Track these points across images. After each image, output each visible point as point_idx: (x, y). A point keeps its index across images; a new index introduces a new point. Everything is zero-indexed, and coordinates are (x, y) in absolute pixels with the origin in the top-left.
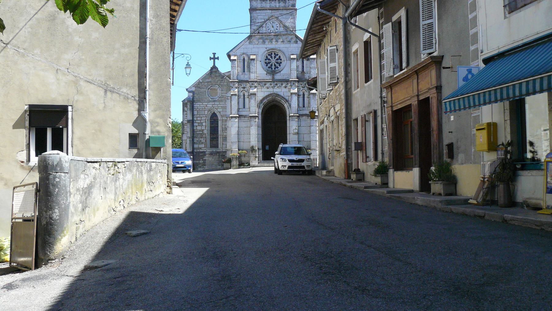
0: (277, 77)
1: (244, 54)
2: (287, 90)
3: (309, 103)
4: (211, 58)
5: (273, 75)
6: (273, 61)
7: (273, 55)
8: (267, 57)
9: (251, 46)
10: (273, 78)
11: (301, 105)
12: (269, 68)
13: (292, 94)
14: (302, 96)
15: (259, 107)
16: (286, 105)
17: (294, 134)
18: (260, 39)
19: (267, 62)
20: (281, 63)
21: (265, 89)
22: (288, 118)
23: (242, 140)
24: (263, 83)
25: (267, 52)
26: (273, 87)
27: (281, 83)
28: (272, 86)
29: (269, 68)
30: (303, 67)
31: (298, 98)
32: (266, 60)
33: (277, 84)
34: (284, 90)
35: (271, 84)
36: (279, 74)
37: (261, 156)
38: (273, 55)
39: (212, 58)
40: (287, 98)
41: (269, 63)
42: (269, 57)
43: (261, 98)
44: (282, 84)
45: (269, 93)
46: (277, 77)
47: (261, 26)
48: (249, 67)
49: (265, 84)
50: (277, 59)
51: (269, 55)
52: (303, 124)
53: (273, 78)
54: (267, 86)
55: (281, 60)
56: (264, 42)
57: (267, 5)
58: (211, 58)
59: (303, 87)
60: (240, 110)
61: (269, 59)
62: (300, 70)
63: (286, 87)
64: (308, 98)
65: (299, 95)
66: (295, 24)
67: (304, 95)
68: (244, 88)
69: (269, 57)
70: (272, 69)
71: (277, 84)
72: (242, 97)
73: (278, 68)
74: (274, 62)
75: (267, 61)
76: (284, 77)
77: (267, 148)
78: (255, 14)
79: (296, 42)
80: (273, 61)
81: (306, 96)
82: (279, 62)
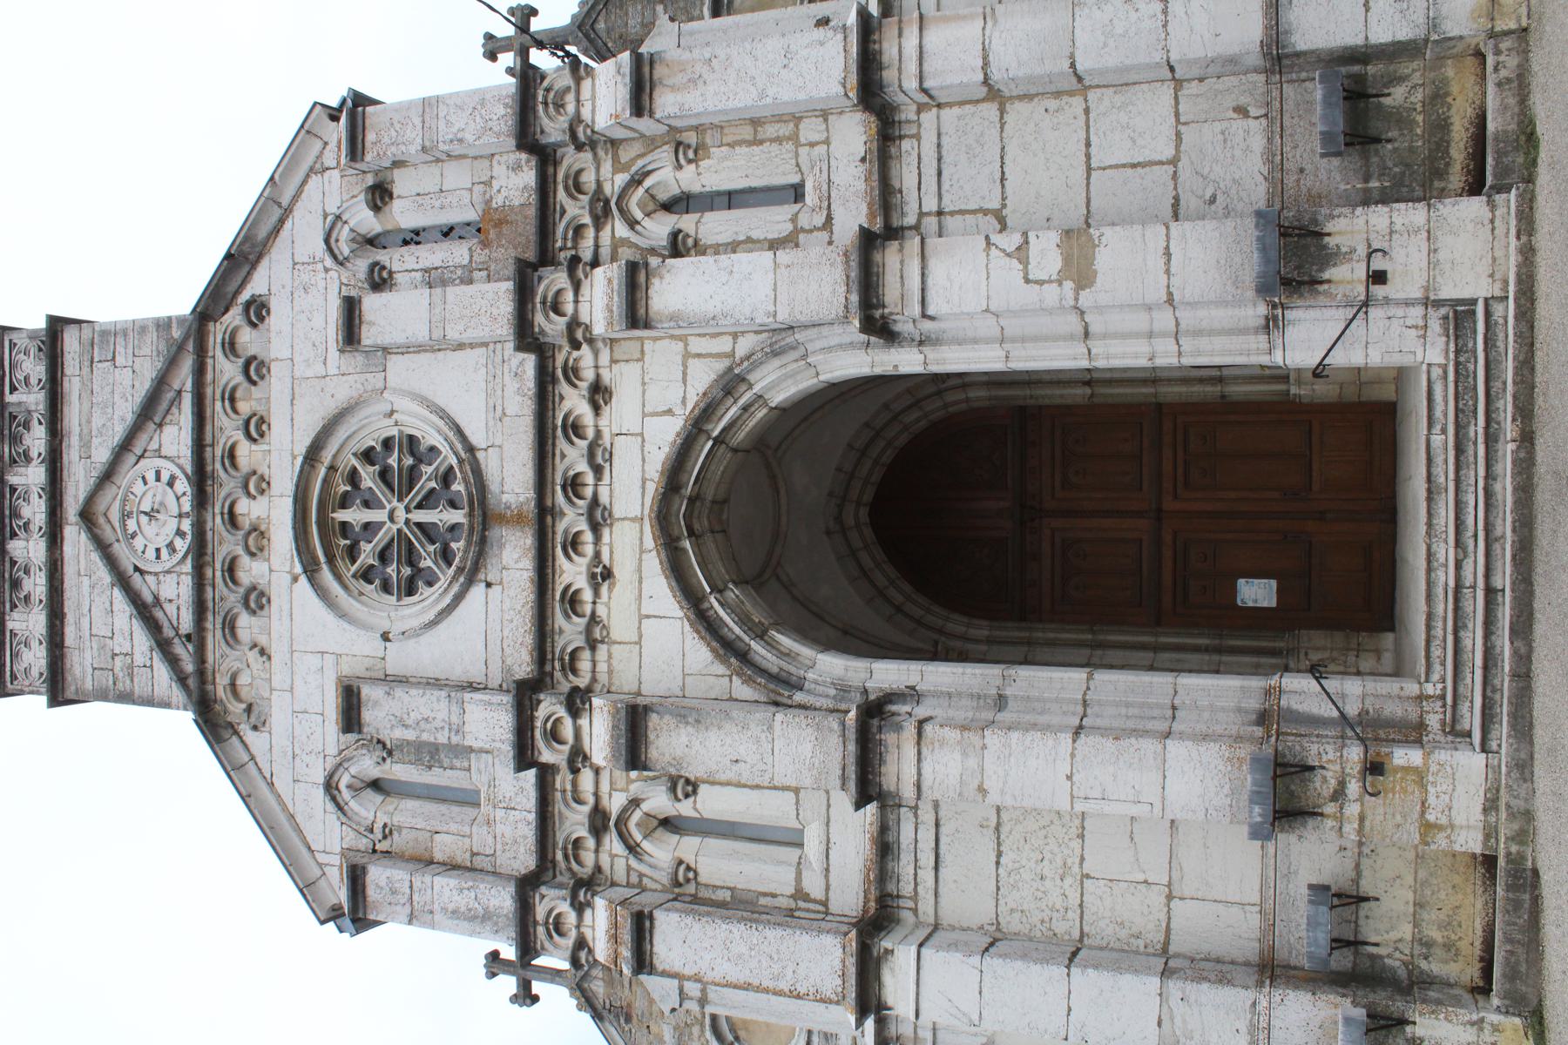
0: (511, 479)
1: (330, 787)
2: (624, 381)
3: (756, 127)
4: (526, 996)
5: (502, 519)
6: (391, 516)
7: (354, 516)
8: (366, 575)
9: (279, 716)
10: (518, 519)
11: (773, 220)
12: (446, 556)
13: (635, 315)
14: (687, 222)
15: (781, 690)
16: (779, 384)
17: (1079, 270)
18: (230, 626)
19: (402, 570)
20: (412, 440)
21: (617, 608)
22: (906, 361)
23: (1140, 913)
24: (559, 620)
25: (326, 575)
26: (598, 517)
27: (562, 444)
28: (583, 525)
29: (446, 556)
30: (447, 232)
31: (699, 249)
32: (386, 587)
33: (573, 485)
34: (622, 414)
35: (573, 544)
36: (490, 464)
37: (1353, 692)
38: (354, 516)
39: (525, 986)
40: (703, 377)
41: (411, 558)
42: (368, 553)
43: (700, 654)
44: (574, 429)
45: (654, 564)
46: (511, 479)
47: (146, 611)
48: (428, 754)
49: (572, 601)
50: (384, 475)
51: (352, 553)
52: (970, 184)
53: (518, 519)
54: (582, 583)
55: (387, 443)
56: (256, 600)
57: (29, 549)
58: (526, 996)
59: (601, 211)
60: (813, 886)
61: (383, 556)
62: (457, 253)
63: (599, 394)
64: (698, 153)
65: (678, 246)
66: (141, 328)
67: (680, 203)
68: (599, 822)
69: (368, 553)
70: (453, 528)
71: (573, 485)
72: (688, 847)
73: (447, 478)
74: (401, 515)
75: (391, 570)
76: (521, 407)
77: (1257, 593)
78: (81, 664)
79: (257, 311)
80: (391, 516)
81: (690, 179)
82: (400, 463)
